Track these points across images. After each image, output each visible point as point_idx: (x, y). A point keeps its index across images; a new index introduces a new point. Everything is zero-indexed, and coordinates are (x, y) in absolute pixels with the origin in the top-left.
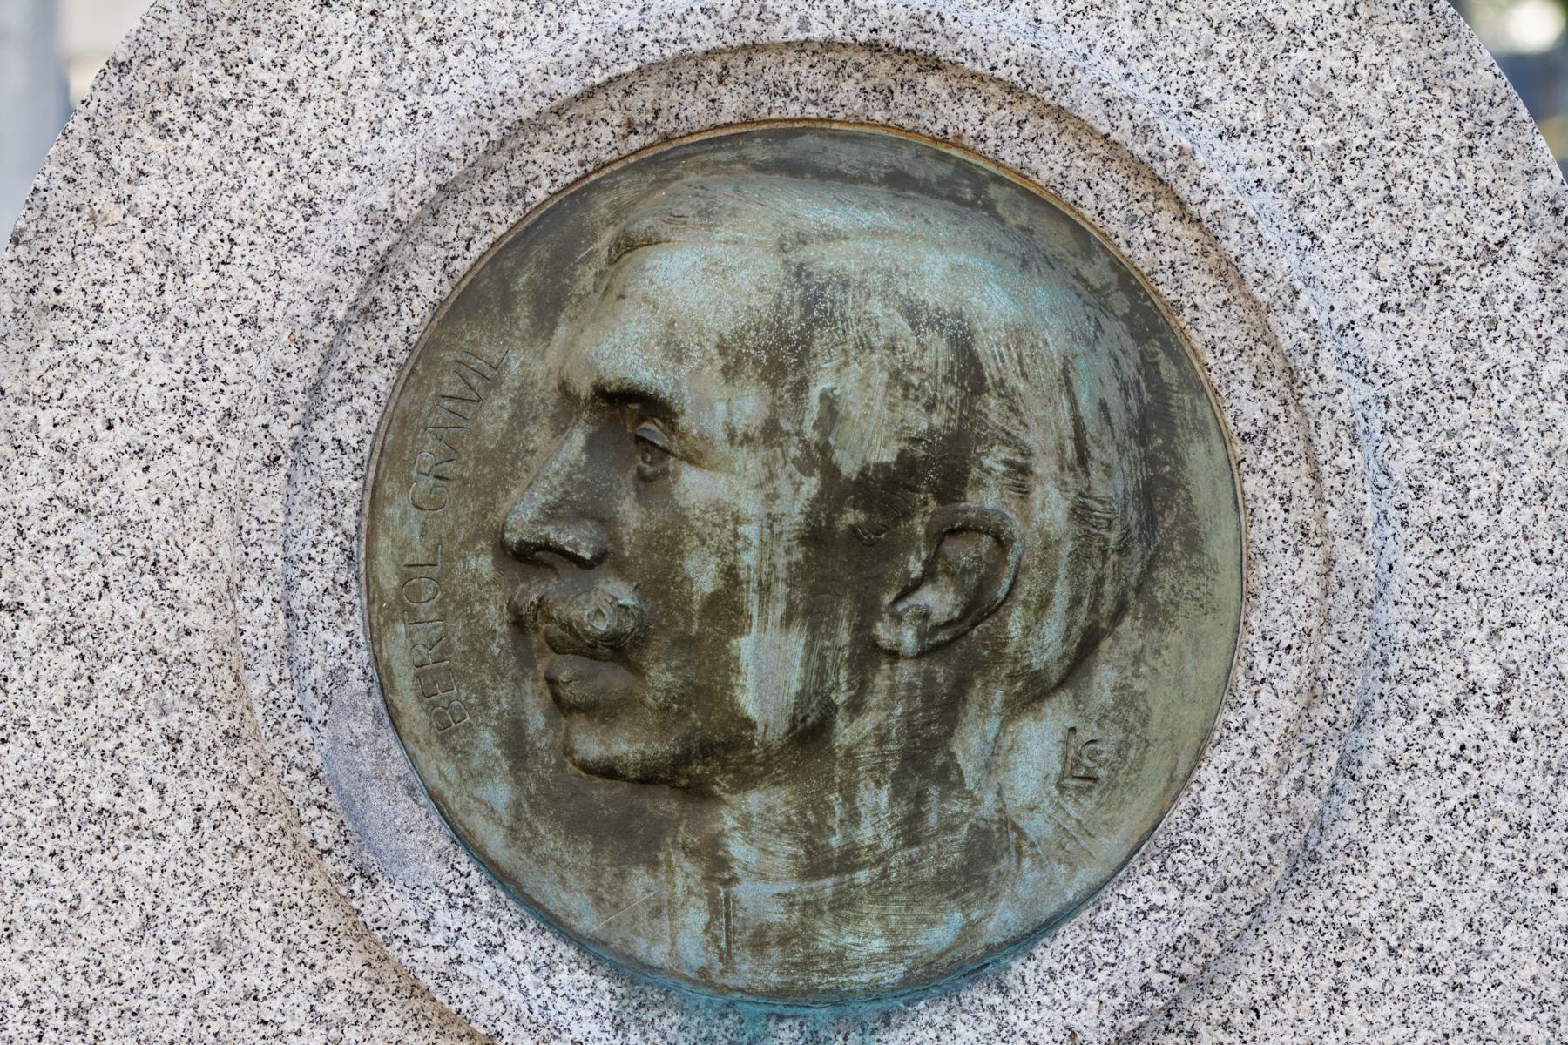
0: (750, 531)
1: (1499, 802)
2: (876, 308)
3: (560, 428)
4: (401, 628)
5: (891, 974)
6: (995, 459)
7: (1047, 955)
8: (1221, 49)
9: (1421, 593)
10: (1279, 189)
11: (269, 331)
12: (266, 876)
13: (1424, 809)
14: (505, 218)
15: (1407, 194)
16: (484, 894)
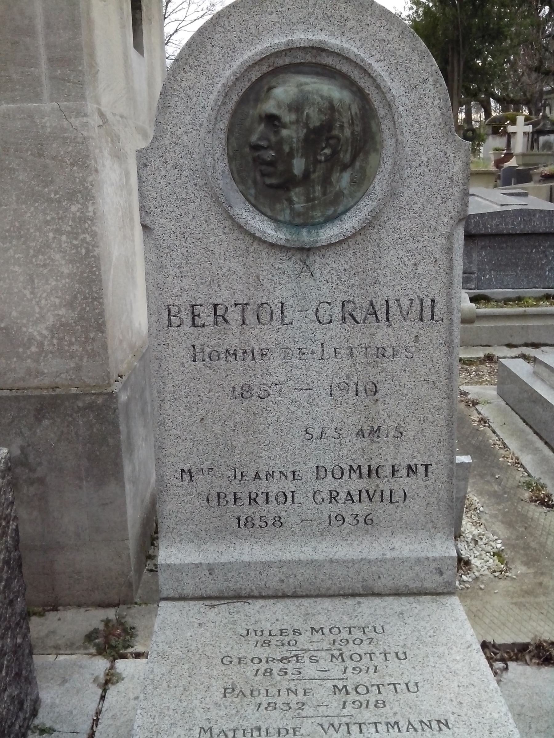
0: (294, 140)
1: (427, 183)
2: (315, 97)
3: (260, 124)
4: (234, 162)
5: (322, 220)
6: (337, 124)
7: (348, 214)
8: (375, 45)
9: (413, 145)
10: (387, 71)
11: (207, 108)
12: (213, 208)
13: (414, 185)
14: (248, 84)
15: (410, 71)
16: (251, 209)
